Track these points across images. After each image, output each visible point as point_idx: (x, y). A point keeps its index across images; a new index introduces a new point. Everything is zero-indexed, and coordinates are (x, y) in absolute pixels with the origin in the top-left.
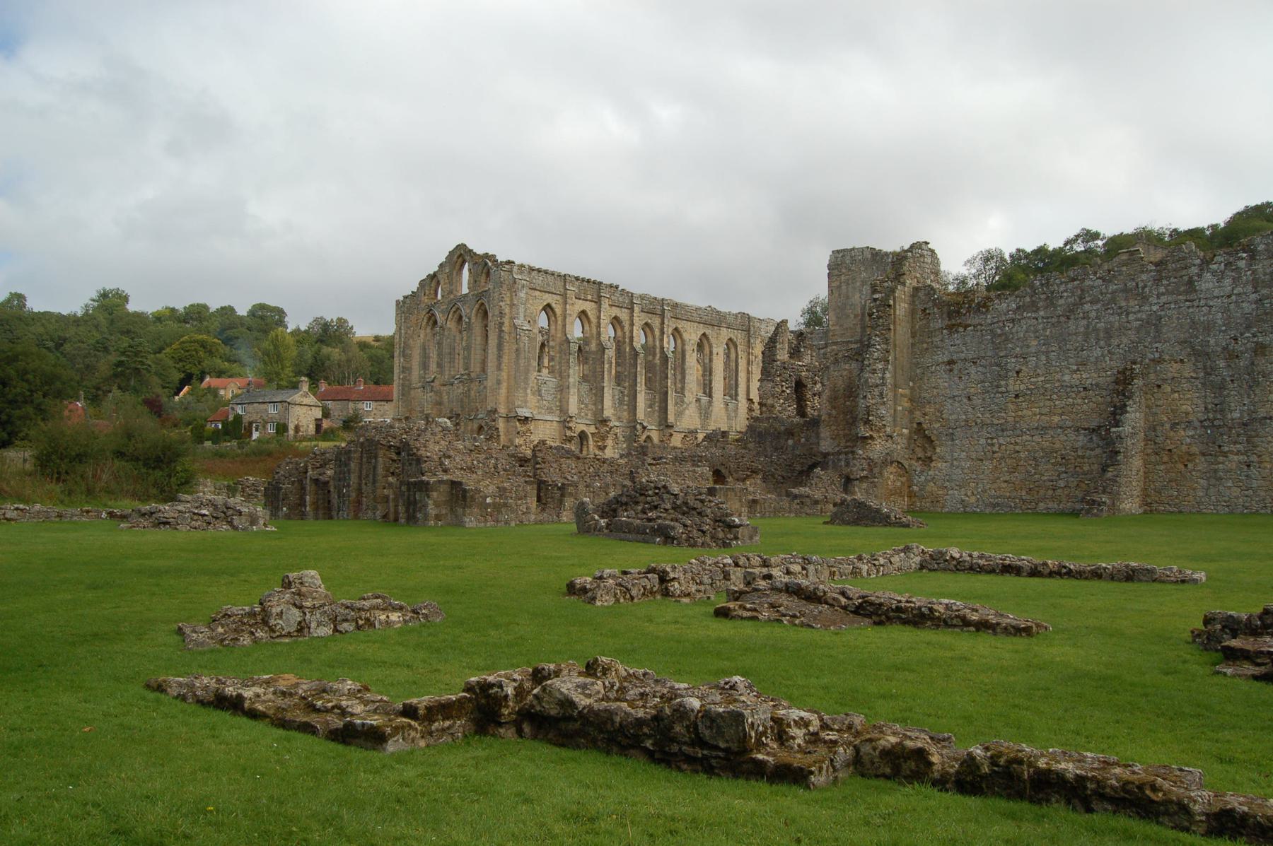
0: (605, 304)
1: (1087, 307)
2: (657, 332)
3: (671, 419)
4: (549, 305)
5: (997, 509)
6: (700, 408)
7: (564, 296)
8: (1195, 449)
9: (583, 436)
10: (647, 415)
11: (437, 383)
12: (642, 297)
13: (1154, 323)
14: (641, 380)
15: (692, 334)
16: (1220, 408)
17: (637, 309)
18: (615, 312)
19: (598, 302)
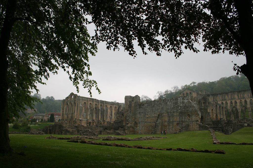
0: (94, 102)
1: (155, 106)
2: (103, 106)
3: (105, 120)
4: (85, 102)
5: (145, 133)
6: (110, 118)
7: (87, 101)
8: (167, 125)
9: (90, 122)
10: (101, 119)
11: (68, 114)
12: (100, 101)
13: (162, 108)
14: (100, 114)
15: (109, 106)
16: (170, 120)
17: (99, 103)
18: (96, 103)
19: (93, 102)
